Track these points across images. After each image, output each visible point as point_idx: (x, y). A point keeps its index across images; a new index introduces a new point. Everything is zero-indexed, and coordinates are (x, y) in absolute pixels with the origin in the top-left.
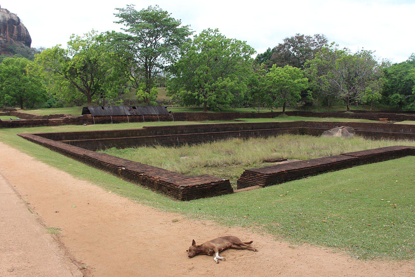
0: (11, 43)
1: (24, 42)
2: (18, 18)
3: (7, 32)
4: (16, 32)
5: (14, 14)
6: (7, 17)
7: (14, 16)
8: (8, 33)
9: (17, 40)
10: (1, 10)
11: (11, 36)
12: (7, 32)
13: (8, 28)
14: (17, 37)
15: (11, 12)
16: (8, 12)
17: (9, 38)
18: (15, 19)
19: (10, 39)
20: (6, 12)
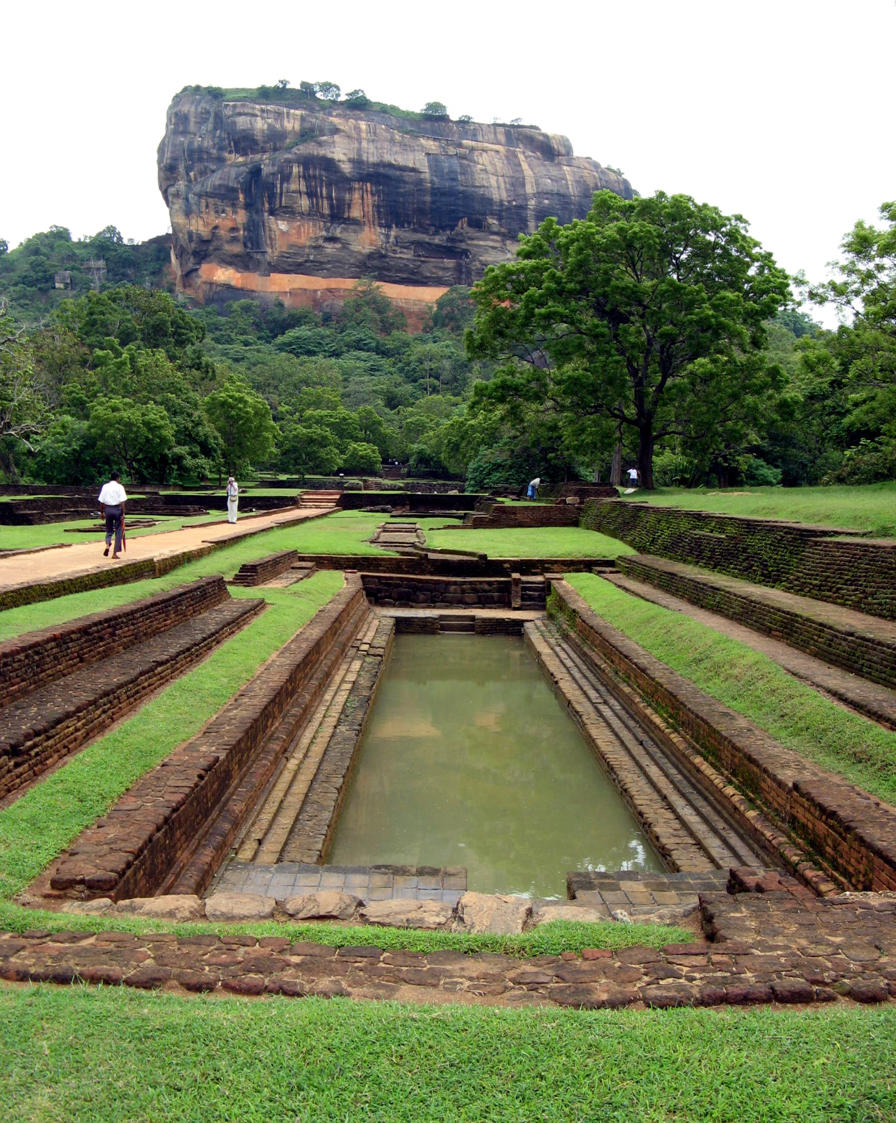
2: (625, 182)
5: (614, 172)
7: (613, 177)
15: (604, 165)
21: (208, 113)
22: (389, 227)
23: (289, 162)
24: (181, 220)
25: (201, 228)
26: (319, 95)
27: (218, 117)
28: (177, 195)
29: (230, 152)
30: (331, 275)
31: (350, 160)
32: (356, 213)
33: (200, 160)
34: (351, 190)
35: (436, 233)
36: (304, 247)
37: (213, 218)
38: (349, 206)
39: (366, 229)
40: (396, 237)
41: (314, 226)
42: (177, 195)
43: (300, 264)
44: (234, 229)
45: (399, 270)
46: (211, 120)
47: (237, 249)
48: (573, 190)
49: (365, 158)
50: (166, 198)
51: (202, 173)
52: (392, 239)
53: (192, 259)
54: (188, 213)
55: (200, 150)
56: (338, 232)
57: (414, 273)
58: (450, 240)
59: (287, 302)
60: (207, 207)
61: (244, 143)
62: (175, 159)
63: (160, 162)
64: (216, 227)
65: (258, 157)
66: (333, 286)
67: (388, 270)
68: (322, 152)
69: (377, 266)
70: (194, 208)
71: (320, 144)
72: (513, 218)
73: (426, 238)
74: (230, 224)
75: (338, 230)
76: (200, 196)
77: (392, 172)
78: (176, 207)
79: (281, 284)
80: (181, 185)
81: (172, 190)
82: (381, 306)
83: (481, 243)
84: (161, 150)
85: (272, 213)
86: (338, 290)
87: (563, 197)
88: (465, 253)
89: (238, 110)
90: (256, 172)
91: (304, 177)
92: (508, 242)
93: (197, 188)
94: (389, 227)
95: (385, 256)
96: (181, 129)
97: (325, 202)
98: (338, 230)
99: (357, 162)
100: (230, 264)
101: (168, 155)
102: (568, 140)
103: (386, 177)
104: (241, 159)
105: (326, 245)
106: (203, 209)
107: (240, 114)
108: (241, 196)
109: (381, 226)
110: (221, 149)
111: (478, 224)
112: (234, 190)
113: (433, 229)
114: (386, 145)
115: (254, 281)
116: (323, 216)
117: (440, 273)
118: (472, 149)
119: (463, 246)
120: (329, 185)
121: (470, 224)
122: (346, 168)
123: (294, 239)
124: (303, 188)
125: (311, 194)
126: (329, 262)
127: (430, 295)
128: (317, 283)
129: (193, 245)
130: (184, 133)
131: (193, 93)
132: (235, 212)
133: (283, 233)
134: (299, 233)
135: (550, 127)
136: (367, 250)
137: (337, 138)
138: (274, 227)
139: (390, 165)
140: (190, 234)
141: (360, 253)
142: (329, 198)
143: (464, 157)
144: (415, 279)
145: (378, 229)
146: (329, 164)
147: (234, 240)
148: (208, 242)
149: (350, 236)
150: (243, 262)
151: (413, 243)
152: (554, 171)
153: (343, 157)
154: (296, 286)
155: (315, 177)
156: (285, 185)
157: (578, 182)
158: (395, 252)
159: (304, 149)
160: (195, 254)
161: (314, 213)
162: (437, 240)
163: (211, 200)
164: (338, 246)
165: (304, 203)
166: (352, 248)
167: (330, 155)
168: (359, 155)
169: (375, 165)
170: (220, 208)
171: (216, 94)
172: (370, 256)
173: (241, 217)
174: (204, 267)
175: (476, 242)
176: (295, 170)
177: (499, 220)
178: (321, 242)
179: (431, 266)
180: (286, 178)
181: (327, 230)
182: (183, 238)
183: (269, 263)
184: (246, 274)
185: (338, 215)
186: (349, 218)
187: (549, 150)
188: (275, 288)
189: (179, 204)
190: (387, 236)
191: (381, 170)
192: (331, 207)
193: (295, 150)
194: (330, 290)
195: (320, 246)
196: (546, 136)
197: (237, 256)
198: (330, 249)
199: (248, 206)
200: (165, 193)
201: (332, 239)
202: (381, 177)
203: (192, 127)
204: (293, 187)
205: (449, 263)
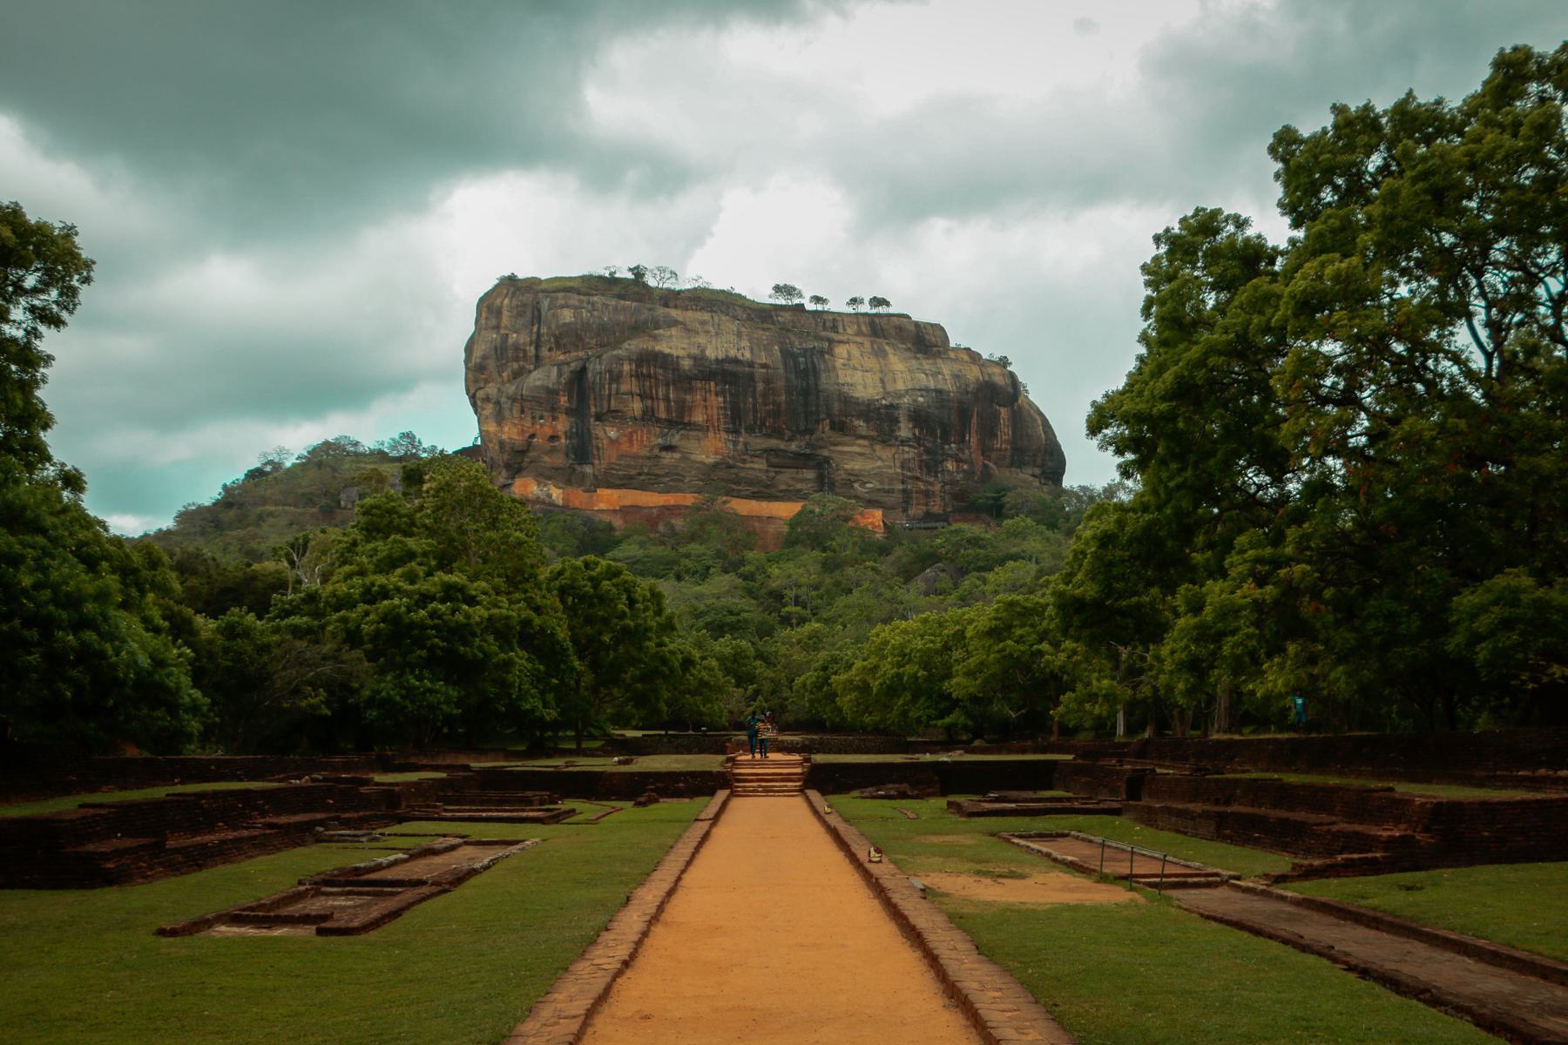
0: (986, 475)
1: (1037, 471)
2: (1012, 374)
3: (973, 434)
4: (1005, 431)
6: (973, 374)
8: (973, 440)
9: (1012, 465)
10: (952, 355)
11: (985, 450)
12: (973, 434)
13: (974, 420)
14: (1008, 454)
15: (985, 356)
16: (974, 357)
17: (979, 460)
18: (999, 380)
19: (985, 466)
20: (966, 358)
21: (525, 305)
22: (737, 432)
23: (620, 359)
24: (492, 427)
25: (515, 437)
26: (652, 282)
27: (537, 309)
28: (487, 399)
29: (550, 350)
30: (668, 490)
31: (689, 356)
32: (699, 418)
33: (517, 359)
34: (691, 390)
35: (790, 440)
36: (636, 457)
37: (528, 424)
38: (690, 409)
39: (711, 434)
40: (745, 444)
41: (649, 432)
42: (487, 399)
43: (631, 478)
44: (553, 438)
45: (750, 483)
46: (529, 314)
47: (560, 460)
48: (950, 387)
49: (708, 353)
50: (474, 405)
51: (517, 375)
52: (740, 447)
53: (504, 473)
54: (500, 418)
55: (516, 348)
56: (675, 440)
57: (767, 487)
58: (808, 444)
59: (618, 522)
60: (522, 412)
61: (567, 338)
62: (484, 357)
63: (467, 361)
64: (533, 436)
65: (581, 354)
66: (672, 502)
67: (736, 483)
68: (657, 348)
69: (724, 479)
70: (507, 413)
71: (655, 338)
72: (880, 419)
73: (782, 445)
74: (549, 432)
75: (677, 437)
76: (513, 399)
77: (740, 369)
78: (486, 412)
79: (607, 500)
80: (491, 390)
81: (480, 394)
82: (729, 523)
83: (846, 449)
84: (469, 349)
85: (599, 417)
86: (678, 507)
87: (939, 392)
88: (827, 460)
89: (561, 302)
90: (583, 370)
91: (637, 377)
92: (878, 447)
93: (511, 389)
94: (737, 432)
95: (730, 467)
96: (493, 322)
97: (662, 405)
98: (677, 437)
99: (699, 360)
100: (549, 478)
101: (478, 353)
102: (942, 329)
103: (734, 375)
104: (562, 357)
105: (664, 454)
106: (516, 412)
107: (562, 307)
108: (563, 400)
109: (727, 432)
110: (538, 347)
111: (840, 427)
112: (552, 393)
113: (788, 433)
114: (733, 338)
115: (579, 498)
116: (658, 420)
117: (799, 486)
118: (830, 341)
119: (825, 453)
120: (668, 385)
121: (832, 428)
122: (686, 364)
123: (625, 447)
124: (636, 390)
125: (642, 396)
126: (667, 475)
127: (786, 510)
128: (652, 499)
129: (506, 457)
130: (497, 328)
131: (510, 283)
132: (554, 419)
133: (611, 441)
134: (631, 441)
135: (922, 314)
136: (711, 460)
137: (674, 331)
138: (601, 434)
139: (736, 361)
140: (502, 443)
141: (703, 463)
142: (667, 399)
143: (822, 352)
144: (764, 492)
145: (724, 436)
146: (664, 361)
147: (553, 450)
148: (523, 452)
149: (691, 445)
150: (568, 477)
151: (765, 451)
152: (927, 365)
153: (681, 353)
154: (627, 503)
155: (649, 376)
156: (614, 386)
157: (956, 377)
158: (744, 461)
159: (635, 345)
160: (508, 466)
161: (649, 416)
162: (793, 447)
163: (527, 404)
164: (677, 456)
165: (637, 406)
166: (693, 457)
167: (667, 351)
168: (703, 351)
169: (717, 360)
170: (538, 413)
171: (532, 285)
172: (715, 466)
173: (562, 425)
174: (518, 482)
175: (840, 448)
176: (626, 368)
177: (867, 421)
178: (656, 451)
179: (785, 478)
180: (616, 378)
181: (664, 436)
182: (494, 446)
183: (595, 477)
184: (570, 489)
185: (679, 421)
186: (689, 424)
187: (924, 341)
188: (602, 506)
189: (489, 409)
190: (735, 443)
191: (727, 366)
192: (668, 409)
193: (626, 345)
194: (667, 508)
195: (657, 456)
196: (917, 324)
197: (556, 469)
198: (668, 458)
199: (569, 412)
200: (473, 399)
201: (669, 448)
202: (726, 375)
203: (506, 319)
204: (624, 388)
205: (810, 474)
